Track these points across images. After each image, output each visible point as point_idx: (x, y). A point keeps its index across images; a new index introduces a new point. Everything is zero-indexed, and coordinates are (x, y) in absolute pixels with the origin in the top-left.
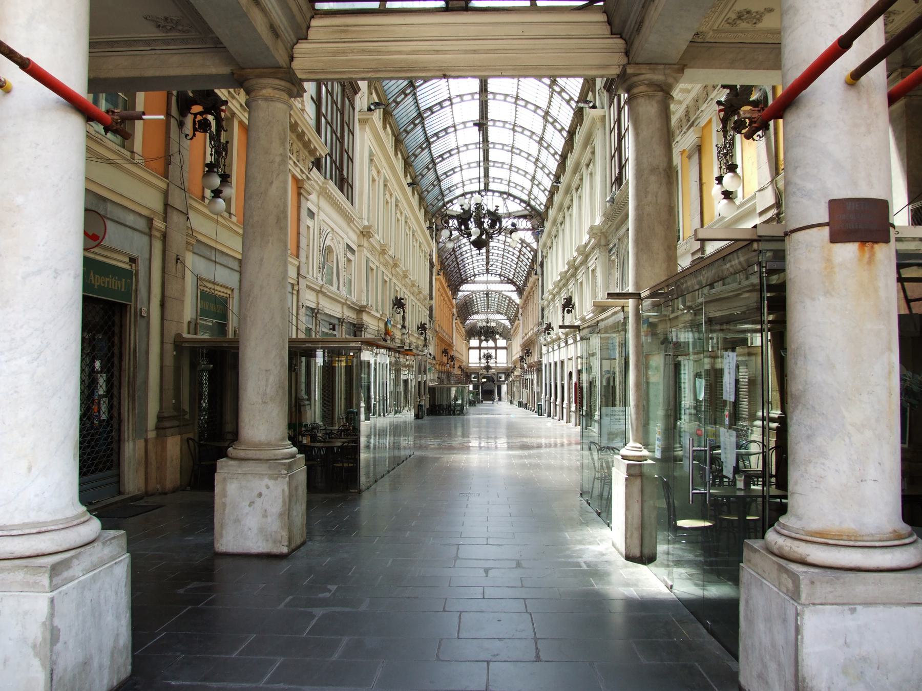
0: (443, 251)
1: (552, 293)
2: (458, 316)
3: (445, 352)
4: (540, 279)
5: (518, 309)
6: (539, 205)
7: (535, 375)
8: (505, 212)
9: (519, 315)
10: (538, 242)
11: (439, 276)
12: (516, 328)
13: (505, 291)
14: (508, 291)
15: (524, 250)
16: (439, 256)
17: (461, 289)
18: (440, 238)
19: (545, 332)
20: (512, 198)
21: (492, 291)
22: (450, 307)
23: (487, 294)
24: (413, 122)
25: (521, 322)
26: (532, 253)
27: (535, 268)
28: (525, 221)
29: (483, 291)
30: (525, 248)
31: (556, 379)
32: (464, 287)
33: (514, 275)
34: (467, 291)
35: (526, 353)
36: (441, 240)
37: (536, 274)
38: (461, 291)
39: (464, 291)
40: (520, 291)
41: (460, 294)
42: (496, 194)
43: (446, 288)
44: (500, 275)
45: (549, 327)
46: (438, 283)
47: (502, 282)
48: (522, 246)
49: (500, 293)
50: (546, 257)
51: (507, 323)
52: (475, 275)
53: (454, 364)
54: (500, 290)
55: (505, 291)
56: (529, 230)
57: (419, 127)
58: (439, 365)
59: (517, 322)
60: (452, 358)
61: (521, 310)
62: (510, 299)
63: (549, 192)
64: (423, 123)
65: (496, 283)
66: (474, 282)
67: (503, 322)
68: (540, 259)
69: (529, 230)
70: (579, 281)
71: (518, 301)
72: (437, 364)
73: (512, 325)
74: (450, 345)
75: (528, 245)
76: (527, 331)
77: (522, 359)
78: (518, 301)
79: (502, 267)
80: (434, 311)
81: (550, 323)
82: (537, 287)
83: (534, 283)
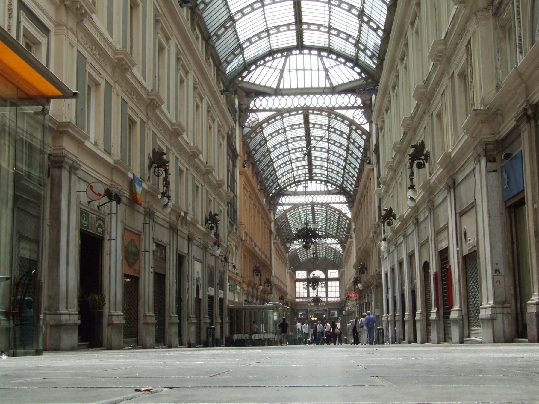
0: (249, 137)
1: (391, 168)
2: (278, 235)
3: (257, 271)
4: (375, 169)
5: (350, 224)
6: (370, 58)
7: (373, 298)
8: (328, 86)
9: (352, 232)
10: (370, 122)
11: (245, 169)
12: (348, 249)
13: (334, 203)
14: (338, 203)
15: (354, 135)
16: (245, 144)
17: (280, 201)
18: (245, 121)
19: (384, 222)
20: (334, 57)
21: (318, 204)
22: (267, 223)
23: (313, 209)
24: (223, 25)
25: (354, 240)
26: (364, 137)
27: (368, 156)
28: (353, 99)
29: (307, 204)
30: (355, 130)
31: (402, 284)
32: (284, 200)
33: (343, 177)
34: (288, 204)
35: (361, 269)
36: (246, 124)
37: (369, 163)
38: (281, 205)
39: (284, 204)
40: (351, 202)
41: (279, 208)
42: (315, 52)
43: (257, 191)
44: (327, 182)
45: (389, 215)
46: (243, 179)
47: (329, 193)
48: (351, 129)
49: (327, 205)
50: (381, 129)
51: (339, 247)
52: (297, 183)
53: (271, 289)
54: (328, 202)
55: (334, 203)
56: (359, 107)
57: (230, 32)
58: (248, 285)
59: (350, 240)
60: (268, 282)
61: (353, 223)
62: (340, 212)
63: (384, 31)
64: (235, 27)
65: (322, 194)
66: (295, 193)
67: (333, 246)
68: (374, 141)
69: (359, 107)
70: (434, 114)
71: (349, 215)
72: (244, 282)
73: (343, 247)
74: (268, 268)
75: (359, 127)
76: (360, 246)
77: (356, 281)
78: (349, 215)
79: (328, 168)
80: (238, 214)
81: (391, 209)
82: (372, 181)
83: (368, 175)
